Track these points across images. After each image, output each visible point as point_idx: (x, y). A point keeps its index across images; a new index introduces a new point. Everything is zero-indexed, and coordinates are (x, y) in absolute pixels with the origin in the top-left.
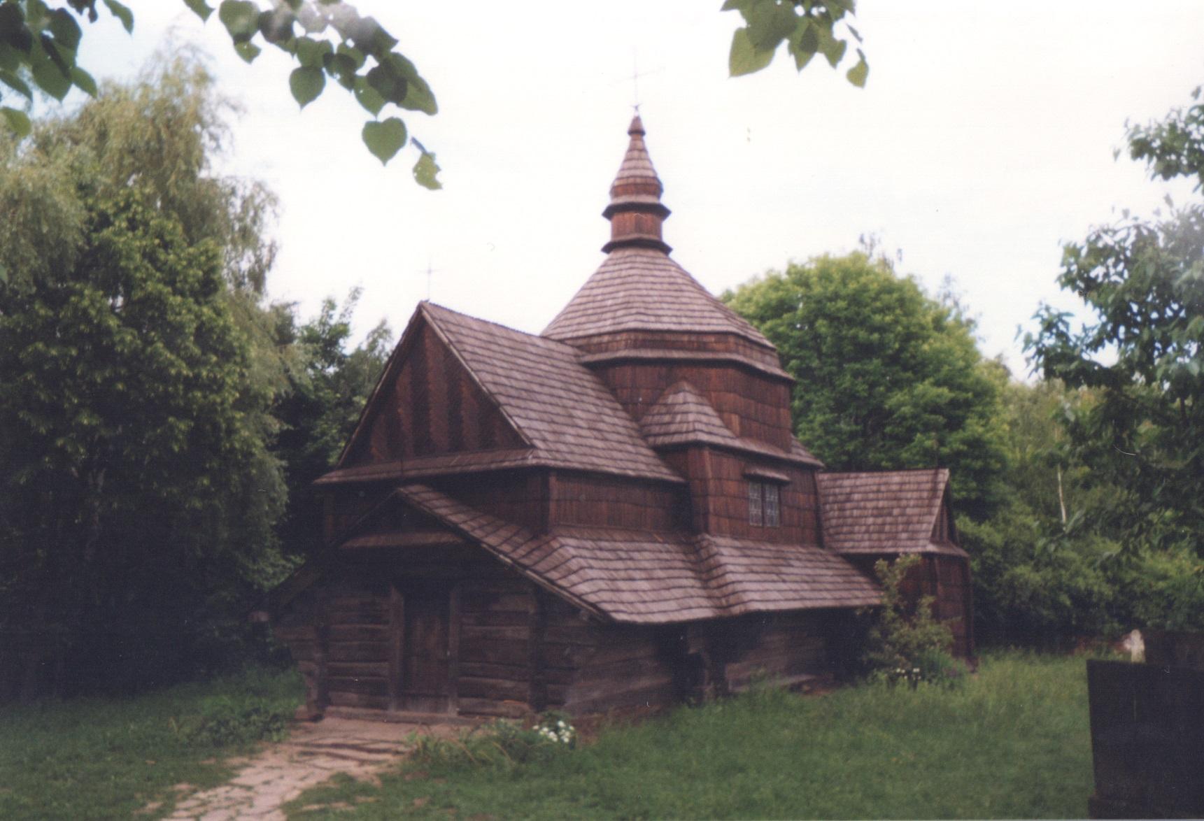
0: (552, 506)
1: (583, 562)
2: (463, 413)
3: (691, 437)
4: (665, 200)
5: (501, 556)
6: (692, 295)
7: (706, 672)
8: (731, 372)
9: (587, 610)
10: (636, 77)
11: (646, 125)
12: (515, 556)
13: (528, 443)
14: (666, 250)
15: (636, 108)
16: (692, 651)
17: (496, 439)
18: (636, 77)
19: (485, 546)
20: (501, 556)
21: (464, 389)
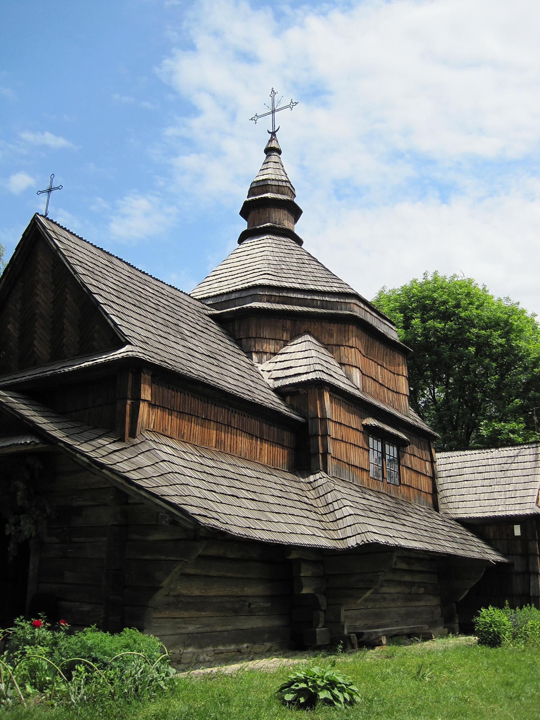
0: (144, 408)
1: (176, 468)
2: (65, 321)
3: (310, 376)
4: (296, 201)
5: (78, 455)
6: (317, 267)
7: (322, 614)
8: (353, 329)
9: (169, 512)
10: (273, 112)
11: (282, 142)
12: (93, 455)
13: (123, 340)
14: (299, 241)
15: (273, 134)
16: (305, 591)
17: (95, 343)
18: (273, 112)
19: (62, 445)
20: (78, 455)
21: (68, 296)
